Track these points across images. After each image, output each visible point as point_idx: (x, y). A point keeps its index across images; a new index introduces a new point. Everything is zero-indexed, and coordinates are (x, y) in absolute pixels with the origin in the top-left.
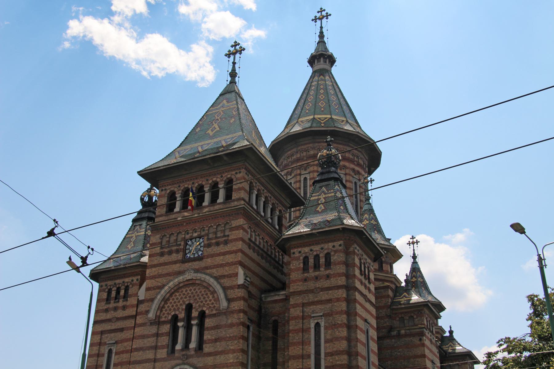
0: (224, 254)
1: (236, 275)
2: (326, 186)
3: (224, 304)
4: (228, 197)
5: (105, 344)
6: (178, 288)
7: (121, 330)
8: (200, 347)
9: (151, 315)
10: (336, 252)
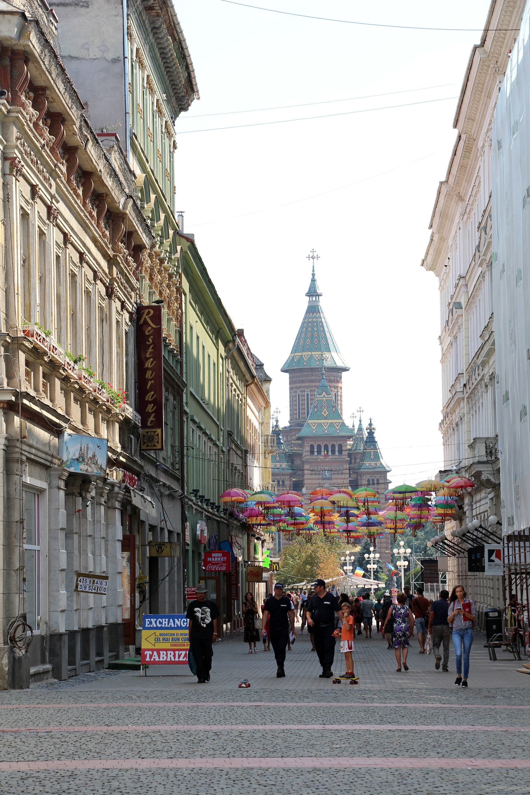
10: (381, 479)
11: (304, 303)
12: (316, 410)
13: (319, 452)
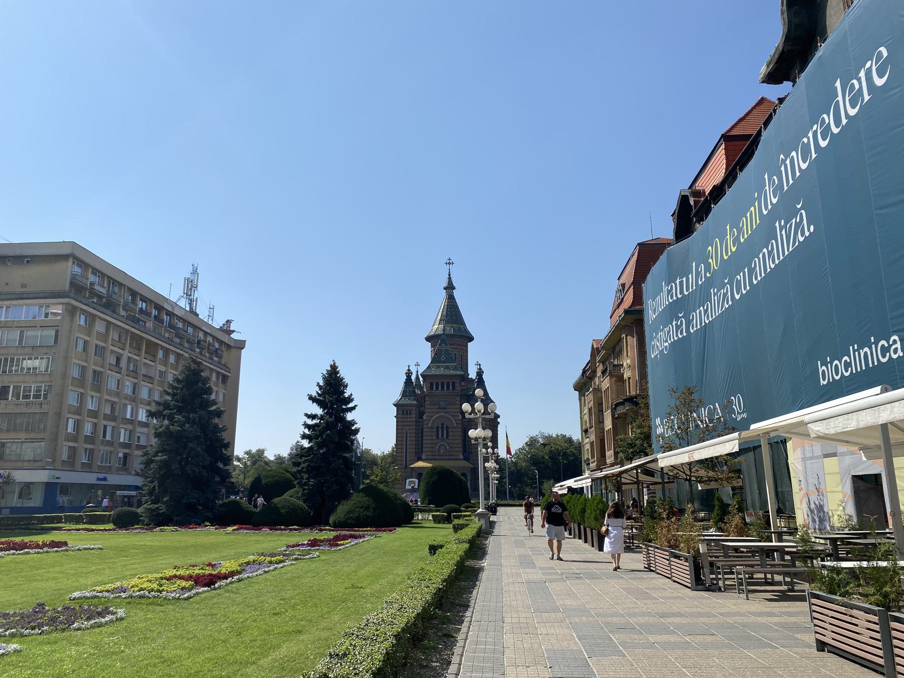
0: (454, 408)
1: (458, 416)
2: (481, 384)
3: (455, 425)
4: (454, 388)
5: (404, 429)
6: (438, 417)
7: (410, 425)
8: (447, 437)
9: (430, 425)
11: (443, 294)
12: (436, 356)
13: (437, 388)
